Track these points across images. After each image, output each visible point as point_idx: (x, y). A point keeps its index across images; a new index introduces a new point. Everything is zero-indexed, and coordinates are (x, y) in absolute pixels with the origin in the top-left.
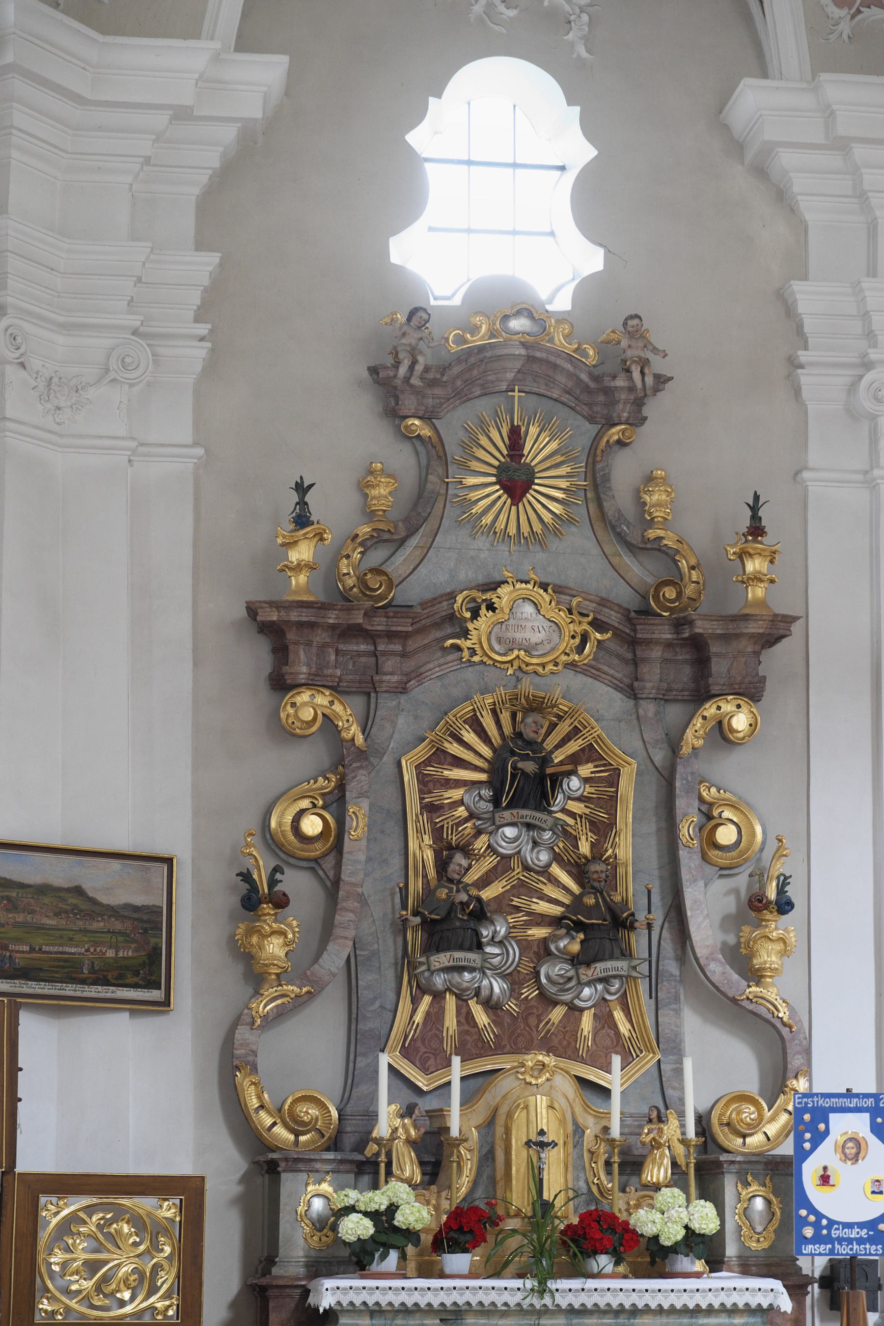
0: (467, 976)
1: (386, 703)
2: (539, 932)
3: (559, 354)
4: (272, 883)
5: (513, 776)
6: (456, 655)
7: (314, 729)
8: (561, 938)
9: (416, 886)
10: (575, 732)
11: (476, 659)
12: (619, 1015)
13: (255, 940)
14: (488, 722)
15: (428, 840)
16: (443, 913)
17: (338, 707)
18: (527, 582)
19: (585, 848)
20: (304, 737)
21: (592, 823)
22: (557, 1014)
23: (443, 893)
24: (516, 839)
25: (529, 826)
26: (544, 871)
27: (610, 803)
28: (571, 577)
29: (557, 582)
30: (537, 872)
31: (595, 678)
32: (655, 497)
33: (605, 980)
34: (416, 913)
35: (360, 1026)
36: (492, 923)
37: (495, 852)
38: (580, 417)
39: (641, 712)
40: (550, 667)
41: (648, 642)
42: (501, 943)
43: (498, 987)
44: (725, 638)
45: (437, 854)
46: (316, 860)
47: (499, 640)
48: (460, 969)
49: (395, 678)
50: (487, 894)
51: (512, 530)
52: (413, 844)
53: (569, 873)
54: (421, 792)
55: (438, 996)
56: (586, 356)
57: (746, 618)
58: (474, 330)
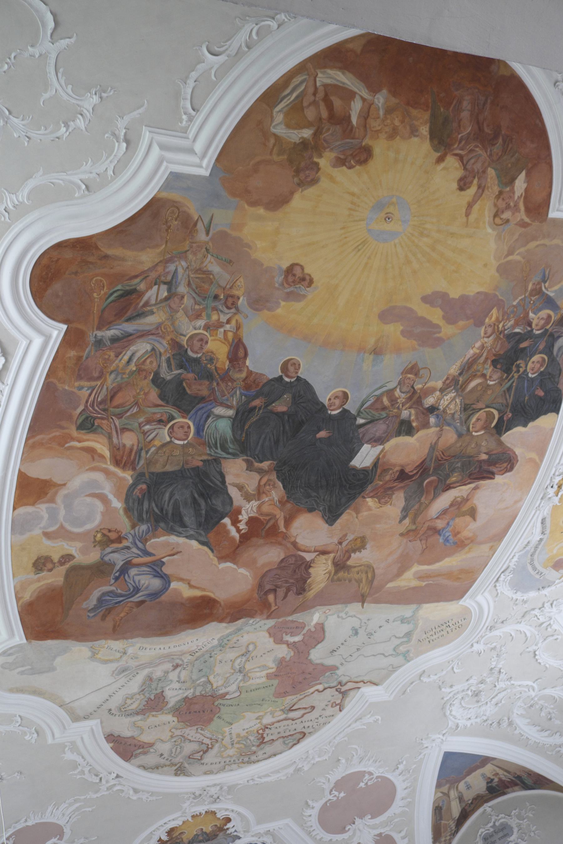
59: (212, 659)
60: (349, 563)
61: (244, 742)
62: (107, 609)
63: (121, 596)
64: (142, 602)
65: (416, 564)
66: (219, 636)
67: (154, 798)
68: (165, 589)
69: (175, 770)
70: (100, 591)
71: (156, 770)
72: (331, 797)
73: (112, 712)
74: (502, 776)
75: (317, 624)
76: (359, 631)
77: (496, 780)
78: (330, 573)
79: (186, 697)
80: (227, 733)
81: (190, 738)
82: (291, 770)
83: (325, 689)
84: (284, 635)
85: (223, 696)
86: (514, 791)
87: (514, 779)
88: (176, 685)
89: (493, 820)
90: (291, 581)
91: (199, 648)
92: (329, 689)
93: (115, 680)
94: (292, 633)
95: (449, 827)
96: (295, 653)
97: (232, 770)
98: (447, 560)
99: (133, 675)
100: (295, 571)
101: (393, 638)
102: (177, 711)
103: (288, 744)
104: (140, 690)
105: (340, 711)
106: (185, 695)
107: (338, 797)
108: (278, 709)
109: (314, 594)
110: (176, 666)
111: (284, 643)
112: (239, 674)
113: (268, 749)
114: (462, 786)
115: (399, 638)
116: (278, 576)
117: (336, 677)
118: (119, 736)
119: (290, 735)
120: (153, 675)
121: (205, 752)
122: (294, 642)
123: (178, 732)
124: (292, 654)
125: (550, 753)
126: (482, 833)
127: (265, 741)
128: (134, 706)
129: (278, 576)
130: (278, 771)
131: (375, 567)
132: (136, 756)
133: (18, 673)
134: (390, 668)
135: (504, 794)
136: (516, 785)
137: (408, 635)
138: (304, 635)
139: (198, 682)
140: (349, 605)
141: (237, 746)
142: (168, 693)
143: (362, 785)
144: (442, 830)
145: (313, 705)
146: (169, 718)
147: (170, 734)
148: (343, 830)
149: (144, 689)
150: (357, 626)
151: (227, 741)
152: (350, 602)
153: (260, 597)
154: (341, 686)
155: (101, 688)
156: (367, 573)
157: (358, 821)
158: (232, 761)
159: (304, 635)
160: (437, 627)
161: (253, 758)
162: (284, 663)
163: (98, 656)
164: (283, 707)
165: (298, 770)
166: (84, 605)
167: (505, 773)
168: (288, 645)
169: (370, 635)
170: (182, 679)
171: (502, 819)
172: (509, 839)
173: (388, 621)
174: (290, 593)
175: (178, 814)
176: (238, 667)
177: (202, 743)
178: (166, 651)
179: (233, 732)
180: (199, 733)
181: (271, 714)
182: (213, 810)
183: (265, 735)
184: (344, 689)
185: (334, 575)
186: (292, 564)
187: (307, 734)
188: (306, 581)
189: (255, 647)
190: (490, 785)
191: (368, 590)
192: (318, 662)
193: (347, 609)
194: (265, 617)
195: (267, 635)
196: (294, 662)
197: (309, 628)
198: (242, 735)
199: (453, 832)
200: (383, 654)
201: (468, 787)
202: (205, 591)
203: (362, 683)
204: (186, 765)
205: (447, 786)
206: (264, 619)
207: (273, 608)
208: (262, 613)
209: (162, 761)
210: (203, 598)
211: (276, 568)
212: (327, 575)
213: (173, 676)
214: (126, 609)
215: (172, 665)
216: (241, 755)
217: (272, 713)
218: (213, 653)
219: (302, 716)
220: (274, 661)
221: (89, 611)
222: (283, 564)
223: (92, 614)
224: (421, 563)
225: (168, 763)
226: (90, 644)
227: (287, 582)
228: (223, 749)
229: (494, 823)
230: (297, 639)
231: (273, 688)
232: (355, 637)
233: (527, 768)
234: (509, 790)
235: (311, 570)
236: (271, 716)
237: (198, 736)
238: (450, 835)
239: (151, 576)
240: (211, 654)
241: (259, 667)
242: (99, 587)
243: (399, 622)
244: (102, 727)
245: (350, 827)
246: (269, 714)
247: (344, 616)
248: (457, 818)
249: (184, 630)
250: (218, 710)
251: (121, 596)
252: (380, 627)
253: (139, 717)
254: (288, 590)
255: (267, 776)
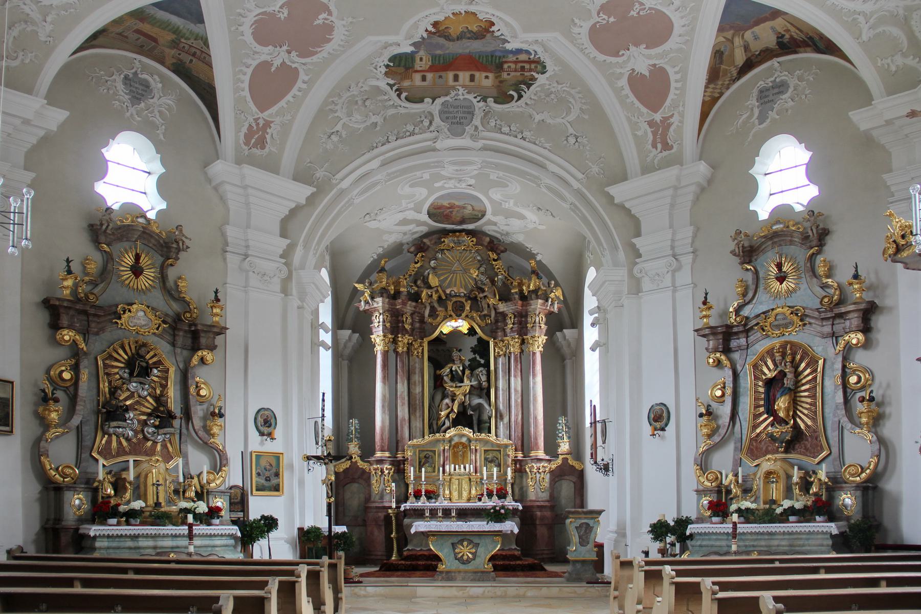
0: (121, 429)
1: (92, 338)
2: (144, 417)
3: (154, 232)
4: (53, 394)
5: (138, 367)
6: (116, 325)
7: (69, 344)
8: (151, 420)
9: (102, 399)
10: (155, 355)
11: (123, 327)
12: (169, 445)
13: (47, 412)
14: (127, 348)
15: (107, 384)
16: (115, 408)
17: (77, 337)
18: (142, 305)
19: (158, 392)
20: (64, 345)
21: (160, 384)
22: (149, 444)
23: (114, 402)
24: (136, 387)
25: (141, 383)
26: (145, 398)
27: (166, 379)
28: (154, 305)
29: (154, 307)
30: (143, 398)
31: (161, 338)
32: (182, 284)
33: (165, 434)
34: (103, 407)
35: (83, 444)
36: (129, 413)
37: (129, 390)
38: (158, 255)
39: (176, 351)
40: (147, 333)
41: (179, 330)
42: (131, 420)
43: (131, 433)
44: (206, 332)
45: (110, 389)
46: (67, 387)
47: (131, 322)
48: (119, 427)
49: (96, 330)
50: (128, 403)
51: (136, 287)
52: (101, 386)
53: (153, 400)
54: (104, 368)
55: (110, 435)
56: (162, 234)
57: (214, 326)
58: (127, 219)
74: (793, 33)
77: (787, 36)
86: (806, 52)
87: (806, 39)
89: (776, 75)
95: (730, 73)
114: (748, 35)
125: (846, 19)
126: (761, 85)
135: (796, 52)
136: (808, 46)
144: (721, 74)
148: (616, 54)
157: (632, 48)
167: (797, 31)
171: (783, 76)
172: (781, 97)
190: (781, 40)
199: (734, 78)
201: (756, 38)
205: (731, 32)
229: (776, 78)
233: (818, 30)
234: (801, 49)
238: (730, 81)
245: (624, 52)
248: (740, 66)
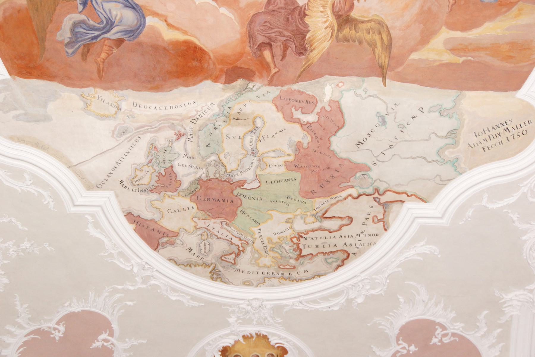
59: (217, 131)
60: (354, 14)
61: (279, 251)
62: (85, 46)
63: (95, 29)
64: (120, 42)
65: (444, 28)
66: (217, 101)
67: (196, 304)
68: (141, 25)
69: (210, 272)
70: (70, 19)
71: (188, 267)
72: (398, 348)
73: (125, 183)
75: (331, 101)
76: (386, 120)
78: (331, 27)
79: (200, 179)
80: (257, 236)
81: (216, 233)
82: (342, 300)
83: (360, 196)
84: (293, 109)
85: (241, 184)
88: (185, 161)
90: (287, 33)
91: (199, 113)
92: (364, 196)
93: (117, 144)
94: (302, 108)
96: (312, 138)
97: (273, 286)
98: (487, 25)
99: (134, 139)
100: (288, 18)
101: (433, 136)
102: (193, 194)
103: (331, 264)
104: (147, 161)
105: (386, 230)
106: (198, 176)
107: (409, 351)
108: (309, 214)
109: (319, 56)
110: (180, 135)
111: (295, 122)
112: (252, 157)
113: (310, 266)
115: (442, 137)
116: (268, 24)
117: (370, 180)
118: (139, 216)
119: (331, 252)
120: (157, 143)
121: (237, 255)
122: (308, 123)
123: (201, 224)
124: (309, 139)
127: (302, 254)
128: (145, 180)
129: (268, 24)
130: (326, 299)
131: (389, 26)
132: (164, 245)
133: (13, 117)
134: (438, 180)
137: (453, 134)
138: (318, 114)
139: (208, 160)
140: (366, 79)
141: (271, 254)
142: (180, 171)
143: (435, 340)
145: (350, 215)
146: (186, 202)
147: (193, 224)
149: (152, 160)
150: (383, 113)
151: (258, 244)
152: (368, 76)
153: (255, 53)
154: (379, 194)
155: (105, 152)
156: (380, 33)
158: (271, 273)
159: (318, 114)
160: (490, 129)
161: (294, 274)
162: (302, 150)
163: (92, 108)
164: (314, 212)
165: (349, 301)
166: (59, 37)
168: (302, 125)
169: (402, 128)
170: (190, 155)
173: (421, 110)
174: (289, 52)
175: (227, 331)
176: (250, 148)
177: (232, 243)
178: (163, 112)
179: (262, 234)
180: (224, 228)
181: (302, 218)
182: (265, 334)
183: (301, 247)
184: (383, 199)
185: (338, 31)
186: (281, 8)
187: (351, 255)
188: (305, 37)
189: (264, 123)
191: (387, 61)
192: (343, 155)
193: (365, 85)
194: (266, 82)
195: (274, 108)
196: (315, 151)
197: (323, 105)
198: (274, 241)
200: (425, 158)
202: (187, 35)
203: (405, 195)
204: (221, 269)
206: (265, 85)
207: (274, 71)
208: (261, 77)
209: (194, 258)
210: (187, 43)
211: (264, 12)
212: (329, 30)
213: (179, 146)
214: (106, 48)
215: (174, 132)
216: (279, 267)
217: (303, 217)
218: (217, 124)
219: (340, 229)
220: (290, 146)
221: (66, 45)
222: (271, 7)
223: (70, 51)
224: (452, 27)
225: (200, 262)
226: (79, 90)
227: (281, 34)
228: (256, 255)
230: (311, 118)
231: (297, 183)
232: (384, 127)
235: (307, 20)
236: (302, 221)
237: (224, 231)
239: (121, 5)
240: (214, 124)
241: (274, 151)
242: (69, 13)
243: (437, 114)
244: (120, 202)
246: (299, 217)
247: (364, 96)
249: (176, 86)
250: (239, 201)
251: (95, 29)
252: (413, 117)
253: (154, 196)
254: (285, 48)
255: (315, 301)
